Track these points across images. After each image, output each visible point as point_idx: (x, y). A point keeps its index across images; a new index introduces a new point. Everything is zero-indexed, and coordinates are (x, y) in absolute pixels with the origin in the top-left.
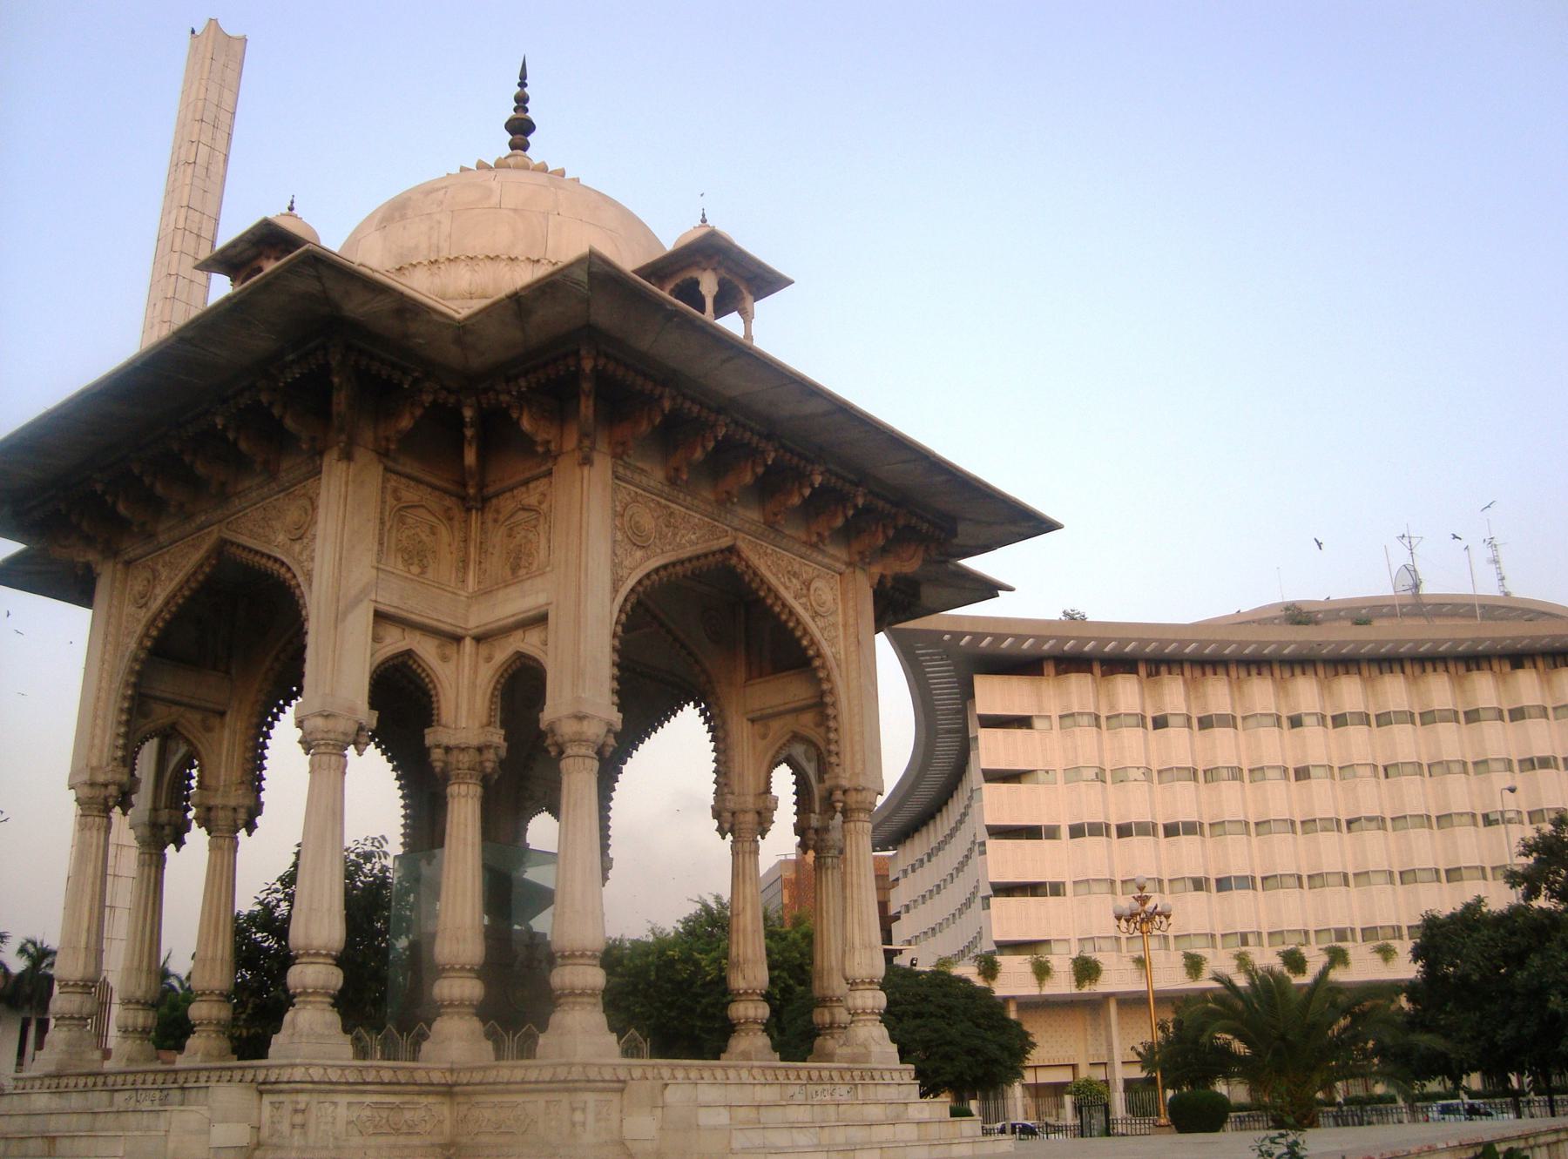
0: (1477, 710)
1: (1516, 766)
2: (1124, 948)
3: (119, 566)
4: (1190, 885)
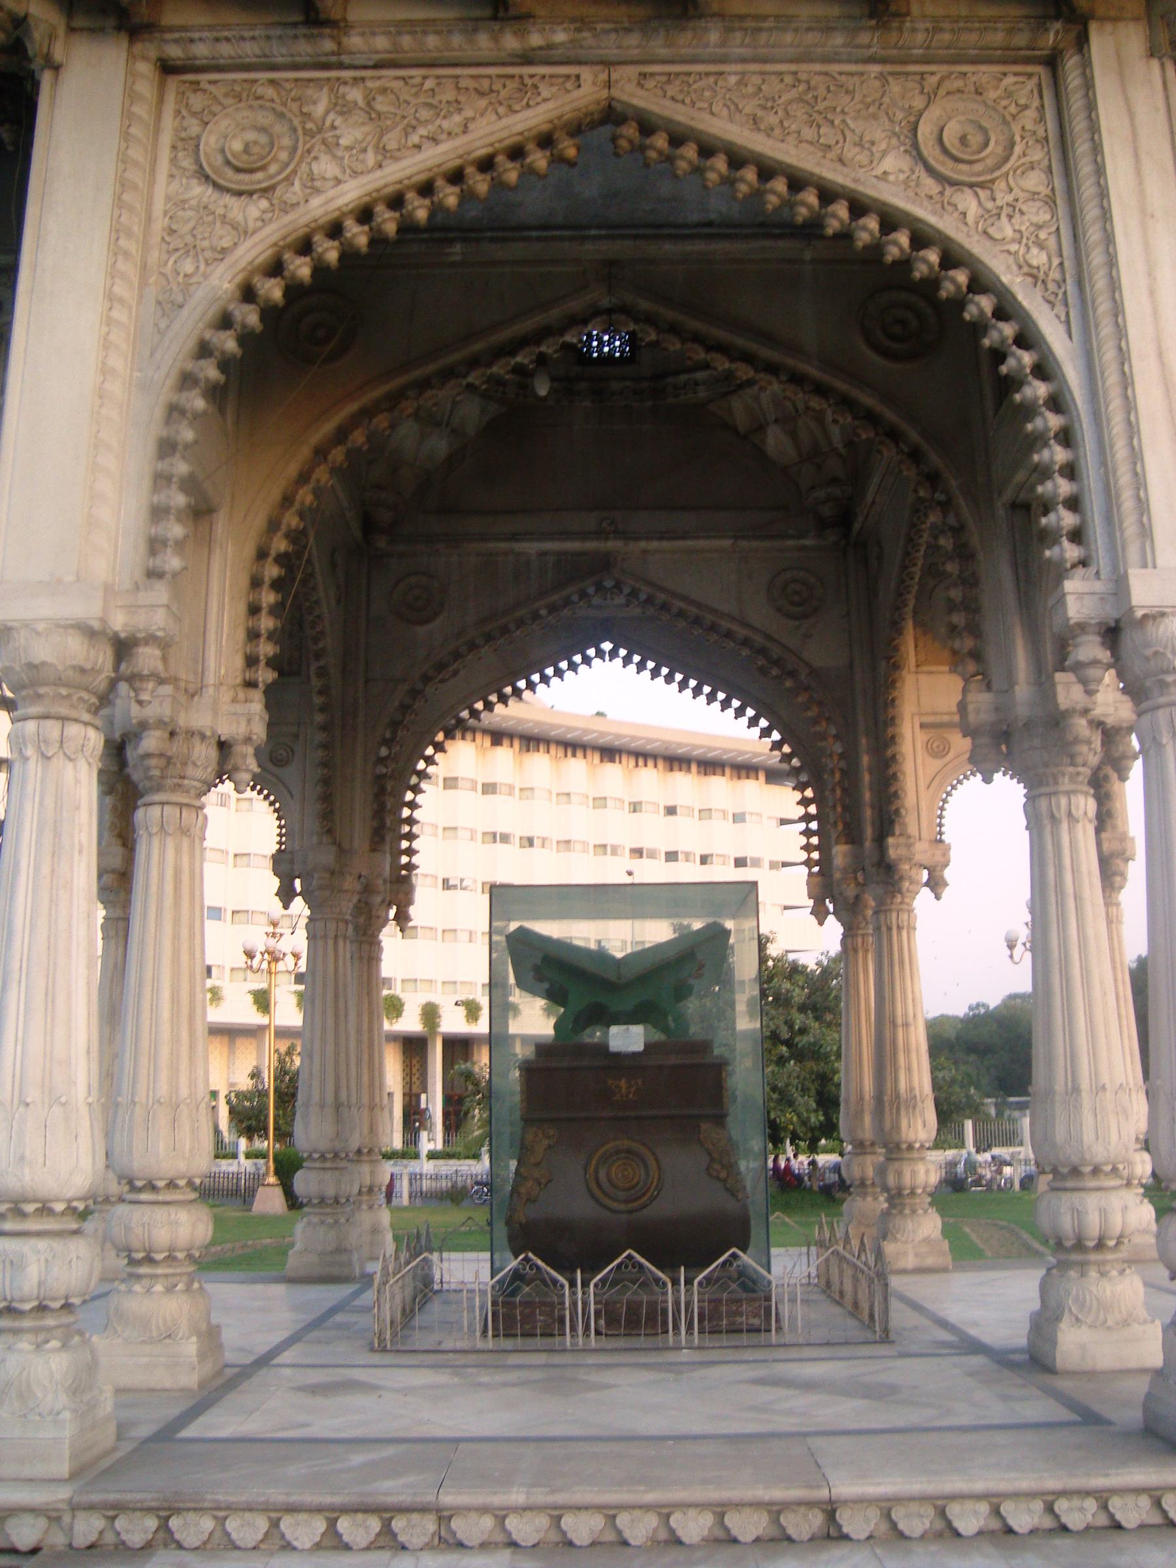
0: (456, 779)
1: (479, 836)
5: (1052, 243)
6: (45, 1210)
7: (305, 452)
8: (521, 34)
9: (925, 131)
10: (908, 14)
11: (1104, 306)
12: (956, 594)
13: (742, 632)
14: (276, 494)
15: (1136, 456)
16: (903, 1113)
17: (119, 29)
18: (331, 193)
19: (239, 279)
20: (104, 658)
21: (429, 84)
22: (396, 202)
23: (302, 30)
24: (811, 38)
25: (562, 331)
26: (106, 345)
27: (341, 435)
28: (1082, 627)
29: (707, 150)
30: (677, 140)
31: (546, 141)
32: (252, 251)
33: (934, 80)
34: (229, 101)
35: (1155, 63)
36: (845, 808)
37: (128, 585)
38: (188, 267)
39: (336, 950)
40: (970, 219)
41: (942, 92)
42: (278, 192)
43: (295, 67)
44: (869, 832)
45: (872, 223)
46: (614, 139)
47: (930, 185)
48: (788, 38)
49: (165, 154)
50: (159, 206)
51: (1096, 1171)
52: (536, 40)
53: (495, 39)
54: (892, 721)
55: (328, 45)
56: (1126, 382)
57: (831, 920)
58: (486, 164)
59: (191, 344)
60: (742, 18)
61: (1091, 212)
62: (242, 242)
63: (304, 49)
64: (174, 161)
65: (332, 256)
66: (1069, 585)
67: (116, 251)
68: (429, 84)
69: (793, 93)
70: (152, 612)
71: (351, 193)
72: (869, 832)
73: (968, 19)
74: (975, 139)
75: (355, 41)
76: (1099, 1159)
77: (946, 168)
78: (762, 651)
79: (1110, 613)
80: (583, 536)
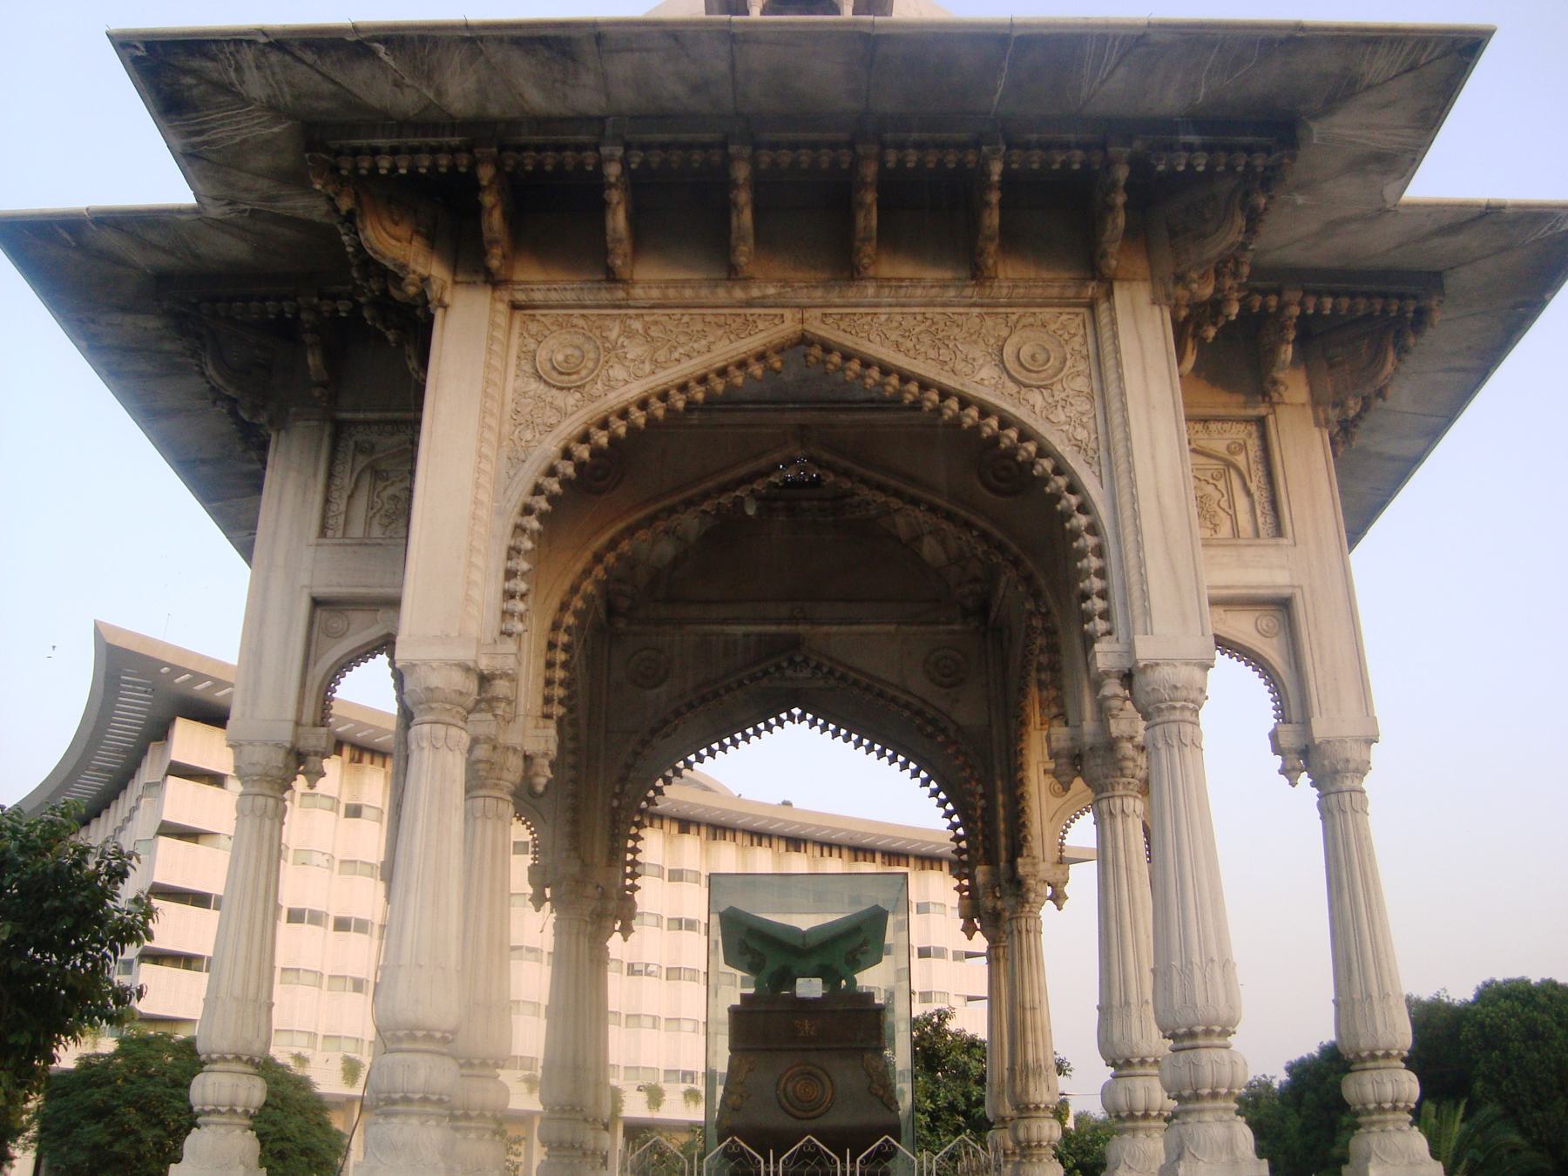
2: (319, 1046)
3: (502, 307)
4: (350, 984)
5: (1091, 425)
6: (429, 1037)
7: (587, 556)
8: (745, 289)
9: (1009, 351)
10: (996, 277)
11: (1123, 466)
12: (1044, 659)
13: (904, 698)
14: (567, 585)
15: (1141, 563)
16: (1031, 1079)
17: (486, 282)
18: (622, 390)
19: (562, 444)
20: (472, 686)
21: (686, 319)
22: (664, 396)
23: (605, 285)
24: (934, 291)
25: (768, 474)
26: (477, 486)
27: (613, 544)
28: (1107, 674)
29: (867, 363)
30: (847, 356)
31: (761, 357)
32: (571, 426)
33: (1014, 317)
34: (554, 328)
35: (1156, 309)
36: (985, 837)
37: (490, 641)
38: (528, 435)
39: (577, 944)
40: (1037, 409)
41: (1020, 325)
42: (588, 387)
43: (599, 307)
44: (1003, 855)
45: (973, 412)
46: (805, 356)
47: (1011, 387)
48: (919, 291)
49: (513, 361)
50: (509, 395)
51: (1143, 1062)
52: (755, 293)
53: (729, 292)
54: (1020, 767)
55: (621, 294)
56: (1136, 515)
57: (978, 935)
58: (722, 372)
59: (530, 486)
60: (889, 279)
61: (1115, 405)
62: (566, 419)
63: (605, 296)
64: (518, 366)
65: (622, 431)
66: (1097, 647)
67: (483, 425)
68: (686, 319)
69: (923, 327)
70: (502, 657)
71: (635, 390)
72: (1003, 855)
73: (1035, 280)
74: (1041, 357)
75: (638, 292)
76: (1144, 1052)
77: (1022, 376)
78: (919, 713)
79: (1125, 665)
80: (779, 622)
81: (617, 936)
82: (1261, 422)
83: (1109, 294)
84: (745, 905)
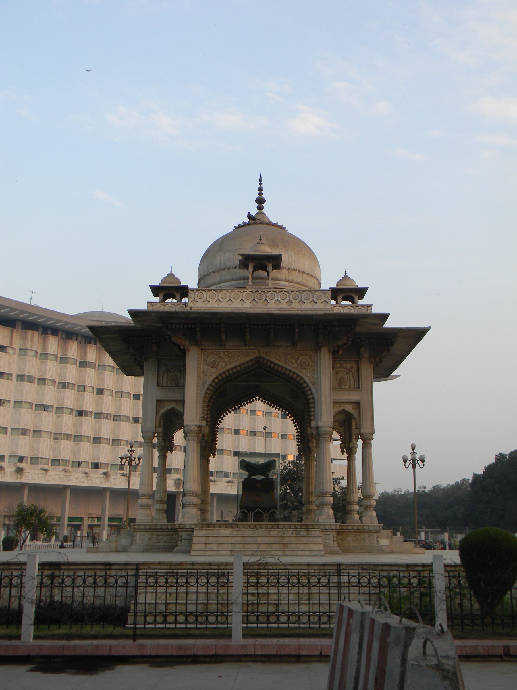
3: (199, 350)
32: (214, 376)
62: (213, 374)
66: (312, 422)
75: (227, 347)
81: (212, 456)
82: (358, 361)
83: (320, 350)
84: (247, 459)
